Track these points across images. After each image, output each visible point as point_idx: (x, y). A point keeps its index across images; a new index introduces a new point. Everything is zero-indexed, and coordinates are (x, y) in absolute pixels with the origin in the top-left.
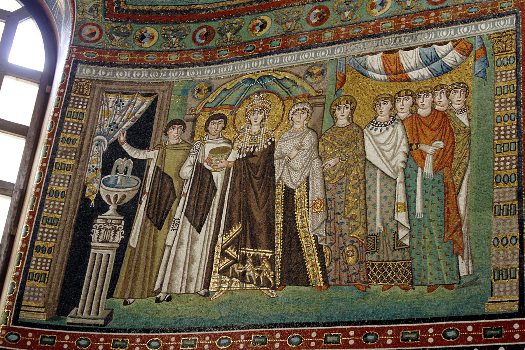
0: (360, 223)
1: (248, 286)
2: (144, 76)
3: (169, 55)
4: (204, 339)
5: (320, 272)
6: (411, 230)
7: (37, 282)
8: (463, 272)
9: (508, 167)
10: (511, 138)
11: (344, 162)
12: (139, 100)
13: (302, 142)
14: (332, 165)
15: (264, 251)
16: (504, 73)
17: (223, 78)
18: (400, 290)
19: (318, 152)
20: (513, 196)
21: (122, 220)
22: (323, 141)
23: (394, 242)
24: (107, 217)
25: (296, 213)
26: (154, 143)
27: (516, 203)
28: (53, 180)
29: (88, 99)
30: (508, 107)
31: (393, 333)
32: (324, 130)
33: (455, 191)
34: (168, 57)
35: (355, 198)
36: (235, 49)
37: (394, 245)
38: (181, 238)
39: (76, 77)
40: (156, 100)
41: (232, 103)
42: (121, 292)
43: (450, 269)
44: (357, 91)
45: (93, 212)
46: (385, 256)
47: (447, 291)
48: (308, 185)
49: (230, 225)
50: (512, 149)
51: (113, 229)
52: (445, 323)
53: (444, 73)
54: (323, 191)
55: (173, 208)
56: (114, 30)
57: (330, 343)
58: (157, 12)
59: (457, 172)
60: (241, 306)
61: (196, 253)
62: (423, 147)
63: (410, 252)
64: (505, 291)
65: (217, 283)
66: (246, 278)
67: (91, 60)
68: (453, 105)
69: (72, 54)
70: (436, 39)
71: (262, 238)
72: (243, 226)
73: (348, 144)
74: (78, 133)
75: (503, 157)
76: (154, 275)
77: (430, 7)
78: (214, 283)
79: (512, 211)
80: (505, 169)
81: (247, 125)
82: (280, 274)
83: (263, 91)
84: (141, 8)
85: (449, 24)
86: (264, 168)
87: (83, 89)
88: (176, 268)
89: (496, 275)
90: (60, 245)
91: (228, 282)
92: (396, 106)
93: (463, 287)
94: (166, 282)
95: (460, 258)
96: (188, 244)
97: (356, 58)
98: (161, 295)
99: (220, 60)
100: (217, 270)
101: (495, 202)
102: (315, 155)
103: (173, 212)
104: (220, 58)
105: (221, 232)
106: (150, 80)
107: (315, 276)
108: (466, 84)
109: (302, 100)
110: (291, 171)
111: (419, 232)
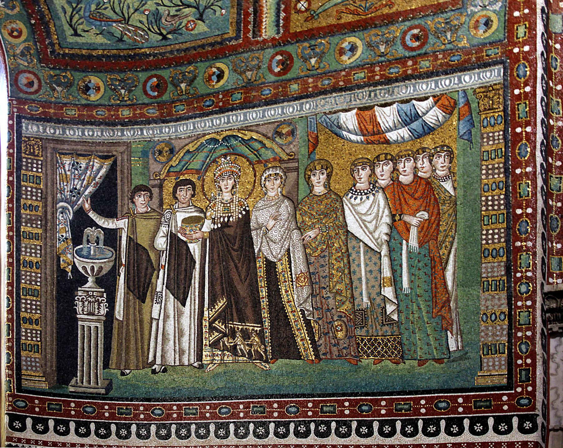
0: (346, 297)
2: (97, 135)
3: (120, 110)
6: (398, 305)
11: (325, 234)
15: (252, 325)
19: (297, 223)
22: (300, 210)
23: (382, 318)
25: (280, 287)
26: (122, 211)
32: (300, 198)
35: (340, 272)
36: (192, 102)
38: (167, 311)
40: (115, 162)
41: (197, 167)
48: (289, 257)
49: (214, 298)
54: (305, 264)
55: (153, 280)
56: (54, 80)
58: (99, 57)
66: (237, 352)
71: (249, 311)
72: (227, 300)
73: (327, 214)
81: (218, 192)
83: (231, 154)
84: (78, 51)
91: (220, 355)
96: (174, 318)
100: (208, 344)
102: (293, 226)
103: (154, 285)
105: (206, 305)
106: (105, 140)
110: (271, 243)
111: (407, 307)
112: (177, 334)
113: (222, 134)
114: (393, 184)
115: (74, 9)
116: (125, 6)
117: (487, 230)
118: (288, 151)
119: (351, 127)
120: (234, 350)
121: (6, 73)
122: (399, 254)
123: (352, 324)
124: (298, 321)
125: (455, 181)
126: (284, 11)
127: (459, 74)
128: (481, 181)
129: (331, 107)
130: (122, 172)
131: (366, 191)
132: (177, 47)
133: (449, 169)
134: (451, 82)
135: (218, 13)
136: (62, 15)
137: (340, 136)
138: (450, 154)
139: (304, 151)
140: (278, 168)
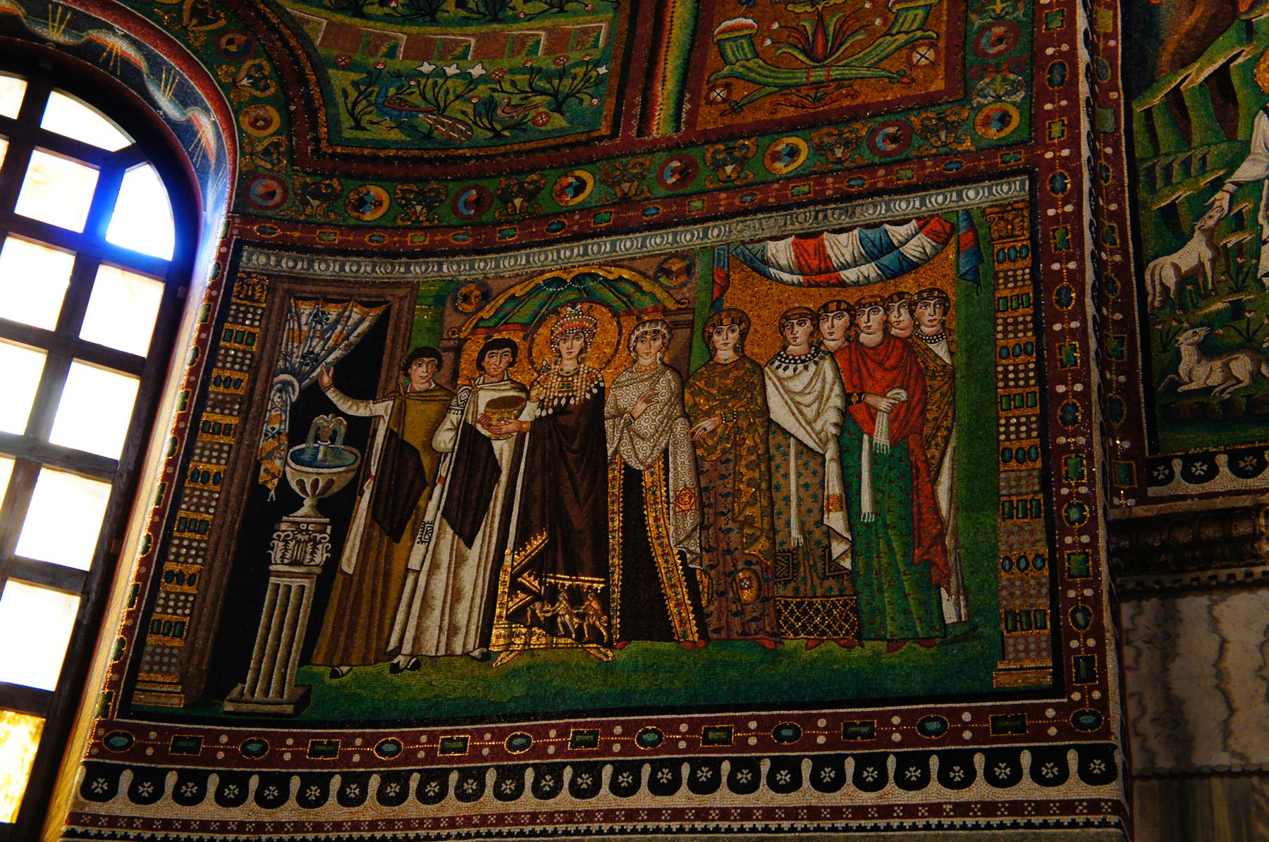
0: (762, 530)
1: (562, 641)
2: (365, 271)
4: (483, 738)
6: (853, 543)
7: (166, 638)
8: (950, 615)
9: (1023, 435)
10: (1027, 385)
11: (730, 424)
13: (653, 389)
14: (709, 429)
15: (590, 579)
16: (1010, 273)
17: (510, 277)
18: (837, 647)
20: (1034, 484)
21: (326, 524)
22: (691, 386)
23: (824, 564)
24: (299, 519)
26: (385, 389)
27: (1040, 496)
28: (198, 451)
29: (263, 309)
30: (1020, 331)
32: (693, 368)
33: (929, 476)
34: (408, 239)
37: (824, 569)
39: (241, 270)
40: (387, 313)
42: (326, 655)
43: (926, 611)
44: (751, 302)
46: (808, 587)
47: (923, 650)
48: (666, 463)
51: (310, 542)
52: (921, 706)
54: (693, 474)
55: (421, 503)
57: (713, 742)
58: (389, 160)
60: (548, 678)
61: (464, 584)
62: (870, 400)
63: (853, 582)
64: (1027, 650)
65: (504, 637)
67: (269, 239)
68: (922, 327)
69: (235, 228)
70: (889, 214)
71: (586, 555)
74: (245, 368)
76: (387, 622)
77: (877, 160)
80: (1018, 438)
83: (582, 302)
85: (909, 189)
87: (254, 290)
88: (429, 610)
89: (1010, 623)
90: (211, 569)
91: (524, 635)
92: (821, 329)
93: (952, 642)
94: (410, 635)
95: (943, 592)
96: (449, 568)
97: (750, 246)
98: (400, 660)
99: (503, 245)
103: (421, 511)
104: (502, 243)
107: (683, 622)
109: (652, 316)
110: (636, 440)
111: (868, 544)
115: (361, 93)
116: (442, 91)
118: (679, 297)
121: (233, 177)
124: (673, 571)
126: (690, 101)
130: (397, 328)
132: (516, 147)
135: (586, 104)
136: (340, 100)
139: (704, 297)
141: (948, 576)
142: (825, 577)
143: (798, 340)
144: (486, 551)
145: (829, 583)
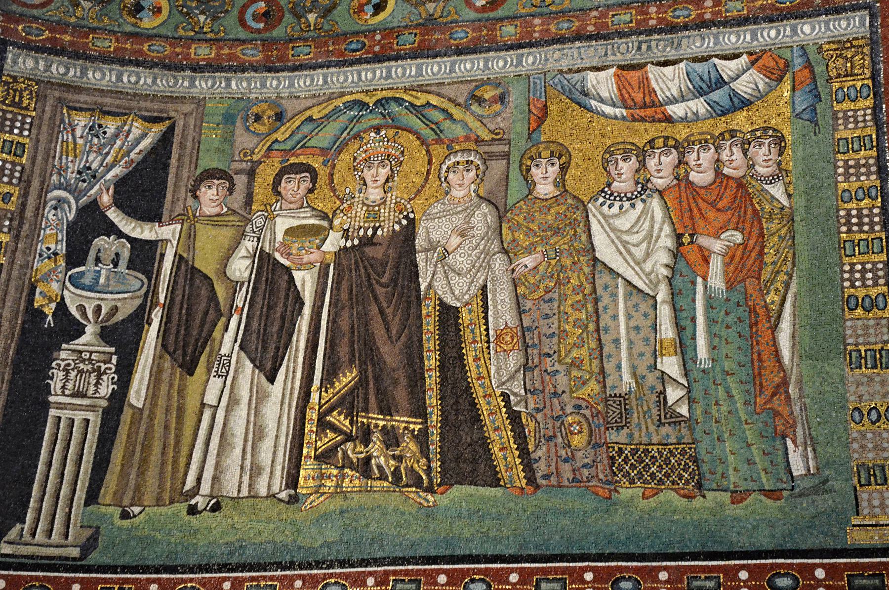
0: (591, 373)
2: (145, 83)
3: (193, 46)
5: (518, 461)
8: (798, 468)
9: (870, 283)
11: (553, 262)
12: (137, 127)
13: (468, 223)
14: (530, 266)
15: (406, 419)
17: (306, 98)
19: (502, 242)
20: (883, 334)
21: (112, 354)
22: (509, 221)
25: (464, 351)
26: (171, 211)
29: (33, 118)
31: (669, 578)
32: (510, 202)
34: (192, 51)
35: (580, 327)
36: (326, 44)
37: (660, 415)
38: (236, 391)
39: (5, 72)
40: (171, 129)
41: (325, 144)
43: (772, 462)
45: (50, 336)
47: (769, 502)
50: (875, 250)
53: (734, 109)
54: (514, 312)
55: (216, 334)
59: (772, 287)
63: (691, 429)
65: (313, 478)
66: (371, 470)
67: (35, 41)
73: (559, 229)
75: (859, 263)
78: (305, 479)
79: (884, 360)
80: (864, 285)
81: (358, 187)
82: (439, 463)
83: (387, 127)
86: (397, 267)
87: (21, 97)
93: (801, 495)
99: (298, 63)
100: (313, 454)
101: (849, 344)
102: (495, 246)
103: (217, 343)
106: (158, 91)
107: (509, 468)
108: (778, 131)
109: (464, 146)
110: (451, 275)
111: (706, 392)
112: (251, 436)
113: (374, 95)
114: (679, 185)
117: (852, 265)
118: (492, 127)
119: (605, 94)
120: (365, 467)
122: (690, 299)
123: (601, 421)
125: (790, 183)
127: (793, 21)
128: (836, 185)
129: (571, 62)
130: (182, 146)
131: (629, 195)
133: (779, 164)
134: (778, 33)
137: (585, 108)
138: (780, 142)
139: (521, 128)
140: (473, 153)
141: (794, 426)
142: (661, 424)
143: (623, 177)
144: (289, 386)
145: (665, 430)
